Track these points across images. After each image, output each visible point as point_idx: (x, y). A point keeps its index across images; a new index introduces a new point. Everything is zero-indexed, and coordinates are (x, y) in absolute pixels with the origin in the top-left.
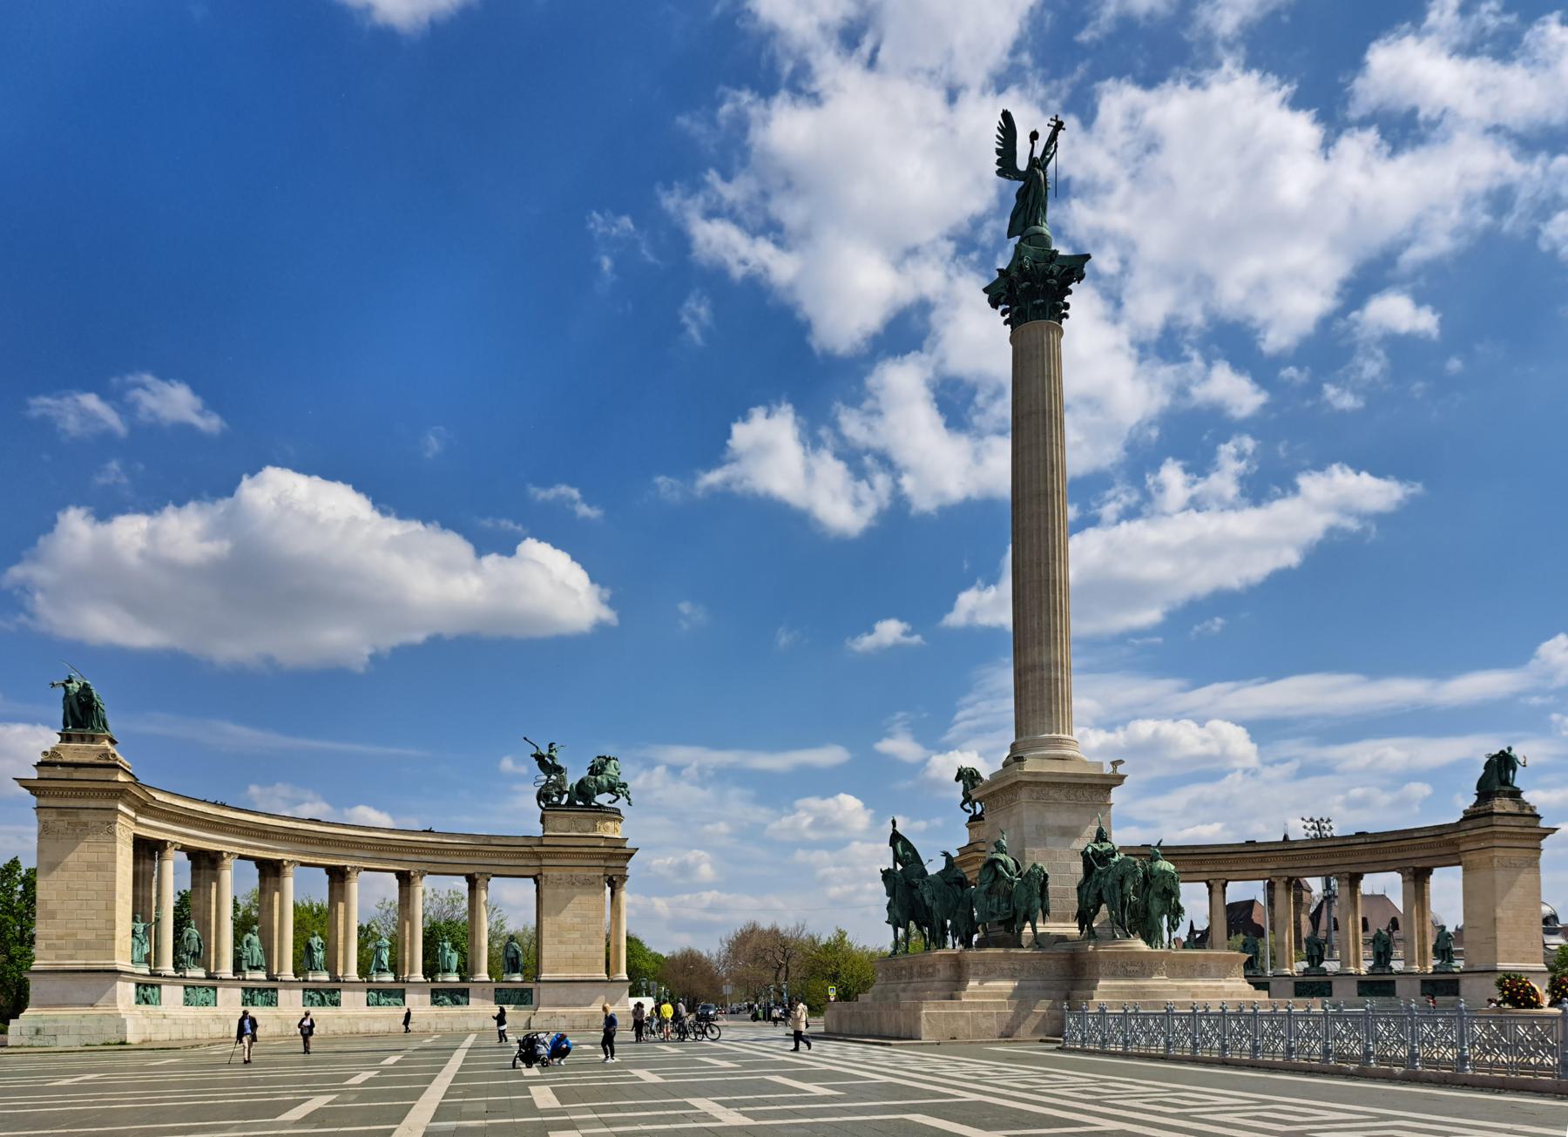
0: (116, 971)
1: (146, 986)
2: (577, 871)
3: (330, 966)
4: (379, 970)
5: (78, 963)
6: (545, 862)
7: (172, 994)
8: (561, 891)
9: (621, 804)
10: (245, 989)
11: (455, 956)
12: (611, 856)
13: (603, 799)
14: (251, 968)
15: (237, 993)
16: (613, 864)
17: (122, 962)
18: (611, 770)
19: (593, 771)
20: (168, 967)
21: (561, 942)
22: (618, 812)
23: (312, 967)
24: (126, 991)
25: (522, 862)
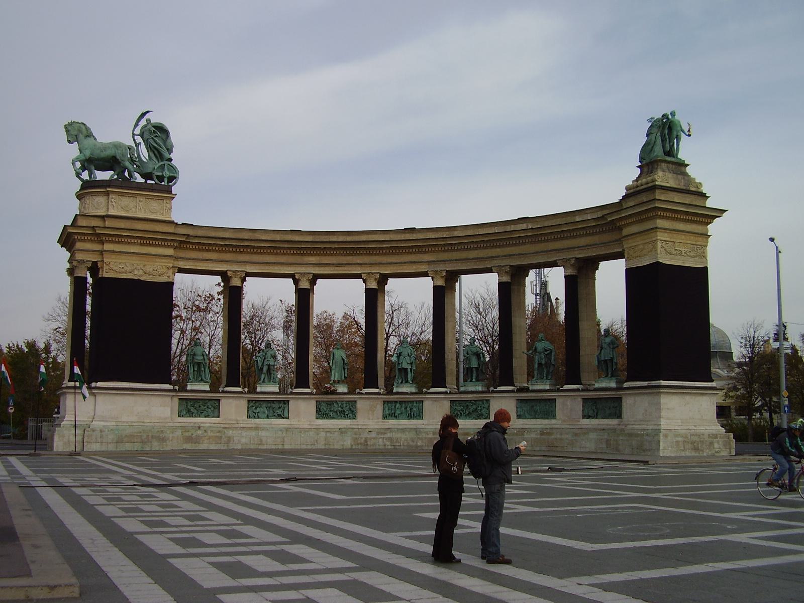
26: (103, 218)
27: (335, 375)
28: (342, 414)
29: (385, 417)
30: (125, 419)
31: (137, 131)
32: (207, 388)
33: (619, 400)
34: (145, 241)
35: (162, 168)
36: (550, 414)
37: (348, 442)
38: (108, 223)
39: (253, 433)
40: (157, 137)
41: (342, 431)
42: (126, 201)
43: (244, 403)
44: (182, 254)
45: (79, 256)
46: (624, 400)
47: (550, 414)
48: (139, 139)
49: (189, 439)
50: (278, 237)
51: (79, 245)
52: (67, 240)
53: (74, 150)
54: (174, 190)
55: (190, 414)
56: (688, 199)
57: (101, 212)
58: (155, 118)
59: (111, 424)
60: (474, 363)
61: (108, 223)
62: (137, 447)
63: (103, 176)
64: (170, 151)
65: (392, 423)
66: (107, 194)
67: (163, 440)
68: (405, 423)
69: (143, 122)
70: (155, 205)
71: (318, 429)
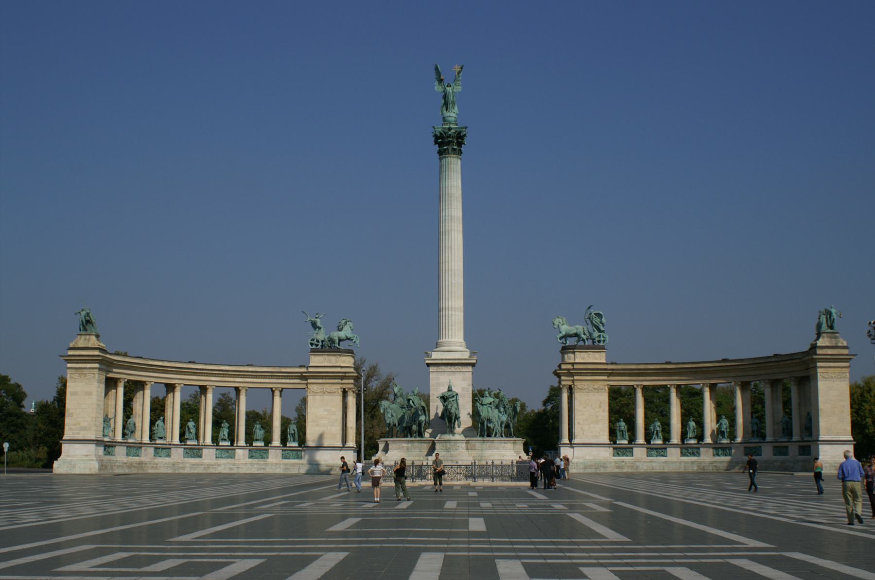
1: (109, 446)
5: (80, 437)
7: (120, 451)
11: (262, 432)
12: (342, 378)
13: (343, 346)
15: (151, 450)
16: (344, 381)
21: (318, 425)
26: (573, 364)
27: (690, 435)
28: (693, 454)
30: (587, 458)
32: (626, 442)
33: (809, 447)
35: (599, 336)
36: (786, 454)
37: (695, 468)
38: (576, 366)
39: (649, 464)
41: (692, 463)
42: (583, 354)
43: (645, 450)
44: (611, 378)
47: (786, 454)
49: (618, 467)
50: (658, 367)
51: (563, 378)
52: (556, 373)
55: (618, 455)
56: (835, 351)
57: (572, 361)
58: (593, 311)
59: (581, 460)
60: (755, 428)
61: (576, 366)
62: (593, 471)
65: (717, 458)
66: (574, 353)
67: (605, 467)
70: (597, 355)
71: (681, 462)
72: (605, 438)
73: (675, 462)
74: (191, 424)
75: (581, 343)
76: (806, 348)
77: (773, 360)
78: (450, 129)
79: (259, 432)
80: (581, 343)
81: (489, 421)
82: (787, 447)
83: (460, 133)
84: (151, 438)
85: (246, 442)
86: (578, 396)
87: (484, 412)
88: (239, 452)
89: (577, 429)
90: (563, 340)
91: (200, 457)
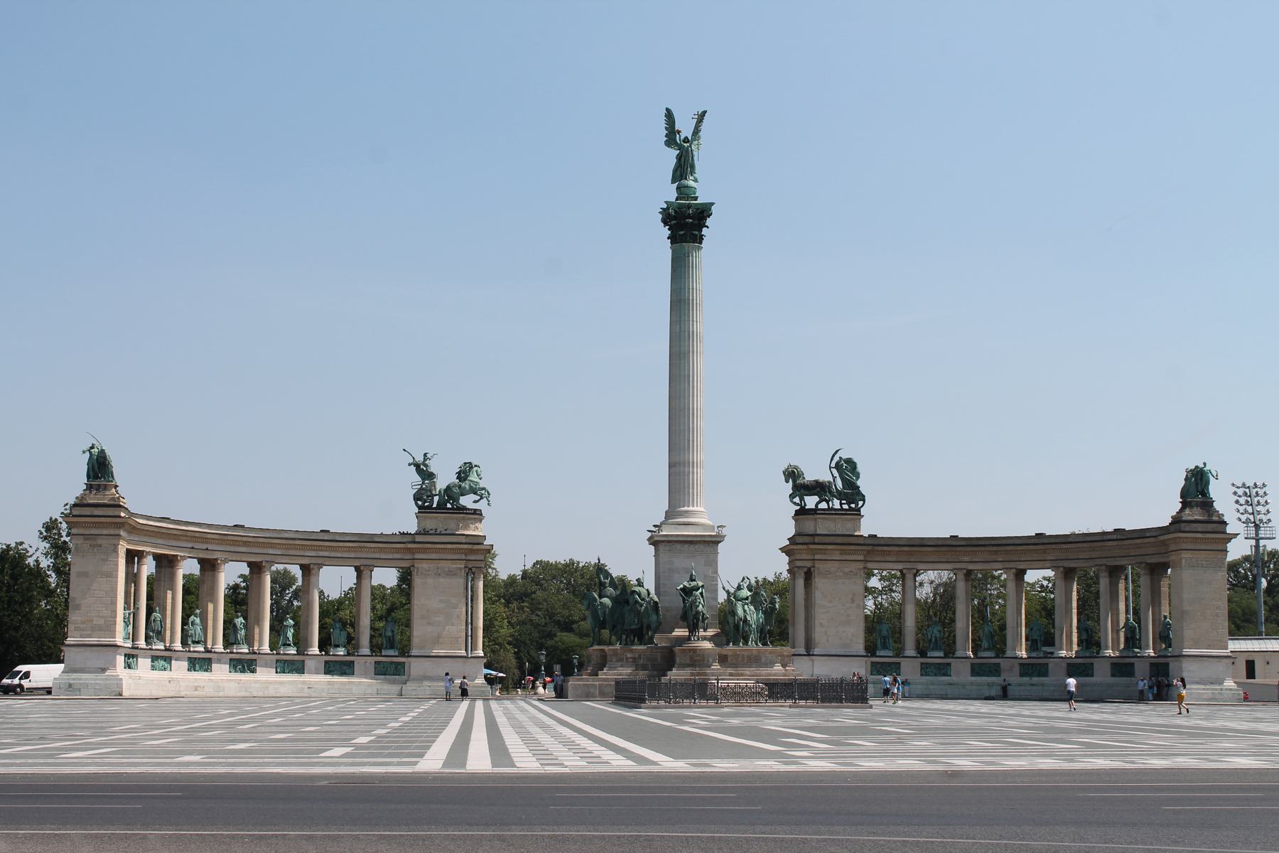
0: (116, 646)
2: (443, 564)
3: (249, 640)
4: (285, 645)
5: (93, 640)
6: (417, 556)
7: (144, 663)
8: (430, 581)
9: (482, 506)
10: (190, 659)
12: (472, 551)
14: (194, 642)
17: (119, 640)
18: (473, 477)
19: (463, 475)
20: (142, 643)
21: (429, 624)
22: (477, 514)
23: (236, 643)
24: (120, 660)
25: (398, 556)
27: (985, 644)
29: (1022, 675)
31: (833, 465)
34: (843, 552)
38: (817, 539)
40: (847, 468)
45: (799, 564)
46: (1171, 666)
48: (835, 471)
53: (789, 487)
54: (863, 511)
56: (1210, 527)
63: (811, 501)
64: (858, 477)
65: (1026, 679)
68: (1035, 679)
69: (836, 459)
70: (849, 525)
72: (860, 647)
73: (964, 686)
74: (239, 621)
75: (823, 505)
76: (1166, 522)
77: (1114, 537)
78: (689, 206)
79: (338, 635)
80: (823, 505)
81: (745, 621)
82: (1133, 664)
83: (702, 212)
84: (184, 643)
85: (321, 648)
86: (819, 583)
87: (740, 612)
88: (309, 664)
89: (818, 634)
90: (797, 500)
91: (253, 671)
